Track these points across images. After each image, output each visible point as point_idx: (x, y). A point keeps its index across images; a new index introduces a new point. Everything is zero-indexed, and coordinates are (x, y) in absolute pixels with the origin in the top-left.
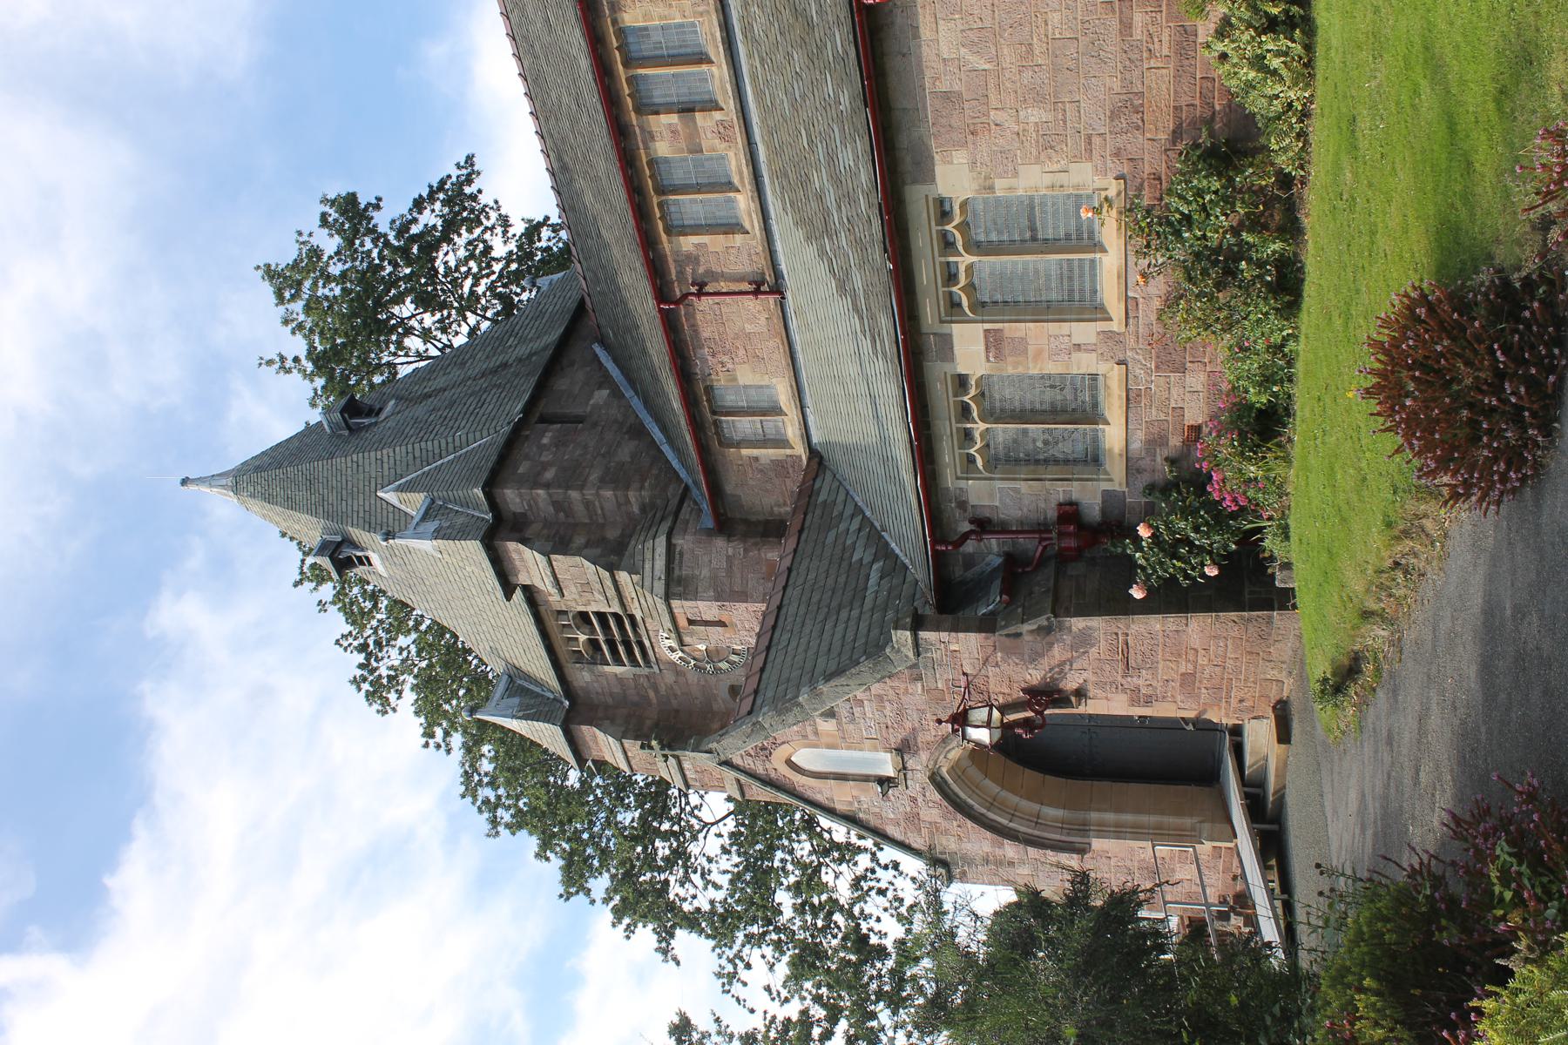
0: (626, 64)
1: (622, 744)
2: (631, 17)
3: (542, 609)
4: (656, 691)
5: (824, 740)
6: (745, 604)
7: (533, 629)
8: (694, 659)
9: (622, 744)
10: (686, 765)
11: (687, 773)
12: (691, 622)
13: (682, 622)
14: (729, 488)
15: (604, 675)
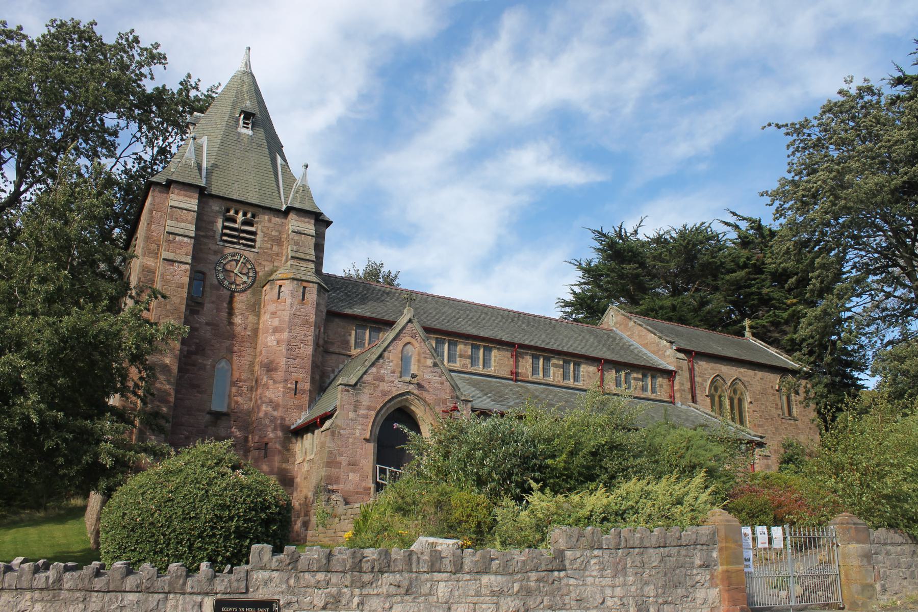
0: (484, 346)
1: (194, 211)
2: (494, 353)
3: (261, 210)
4: (203, 236)
5: (422, 360)
6: (314, 313)
7: (254, 202)
8: (226, 264)
9: (194, 211)
10: (186, 239)
11: (180, 237)
12: (304, 288)
13: (305, 284)
14: (337, 320)
15: (217, 217)
